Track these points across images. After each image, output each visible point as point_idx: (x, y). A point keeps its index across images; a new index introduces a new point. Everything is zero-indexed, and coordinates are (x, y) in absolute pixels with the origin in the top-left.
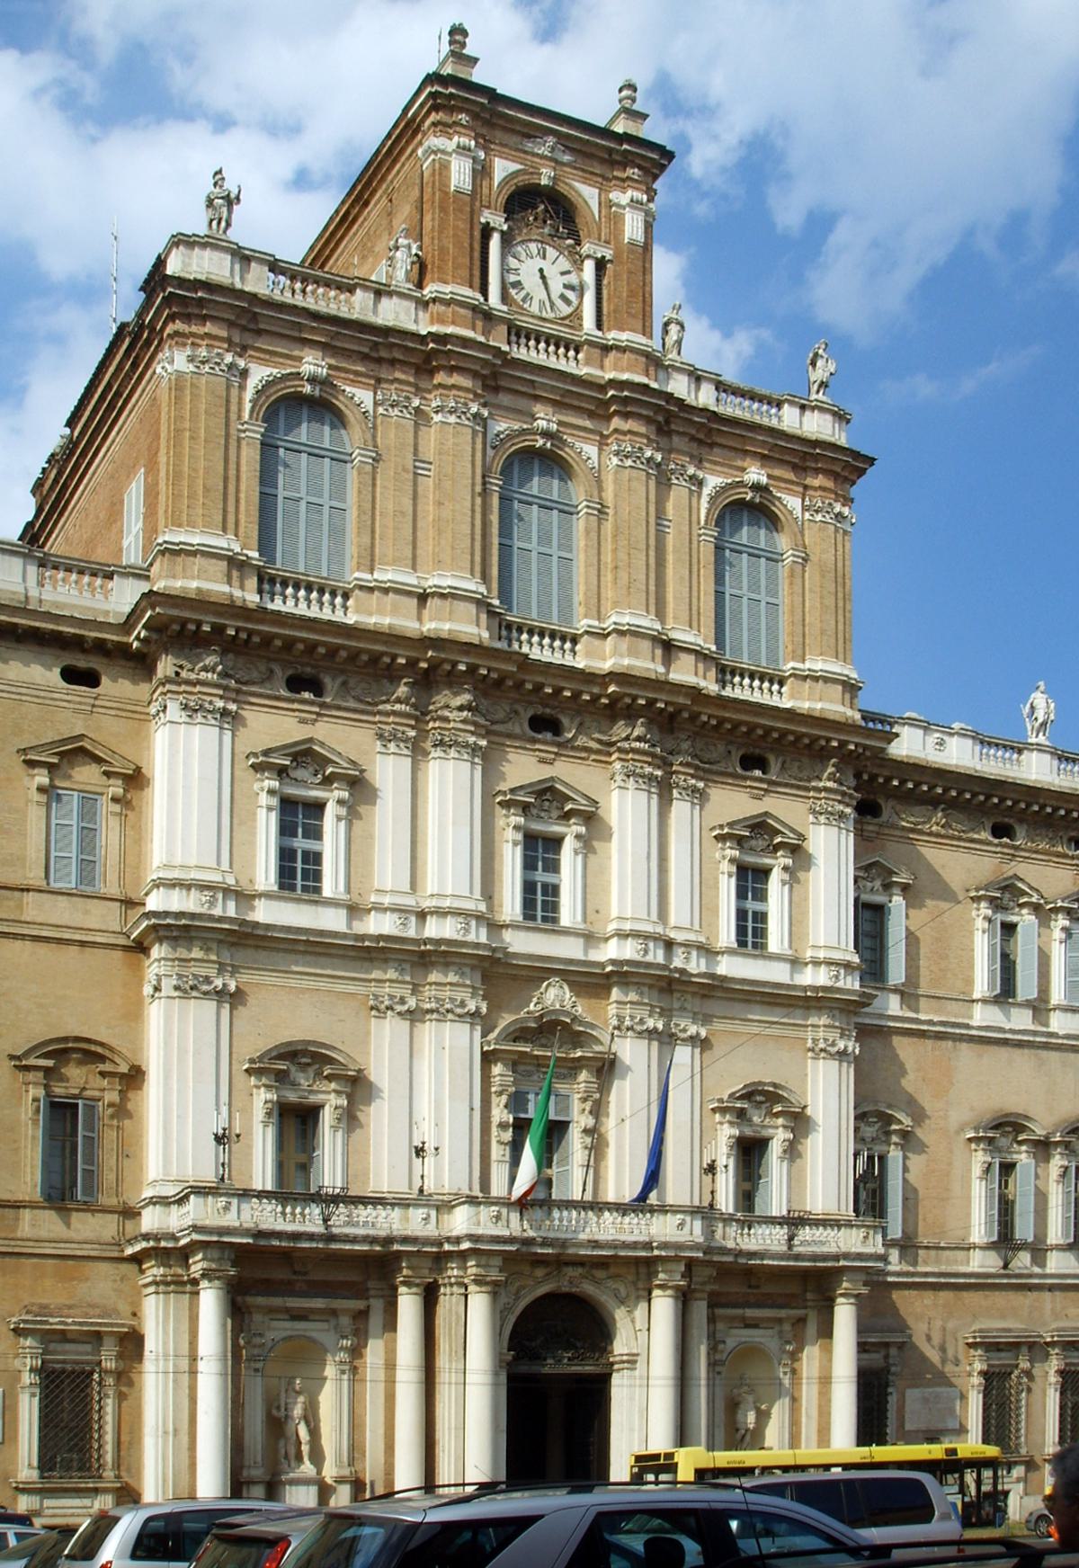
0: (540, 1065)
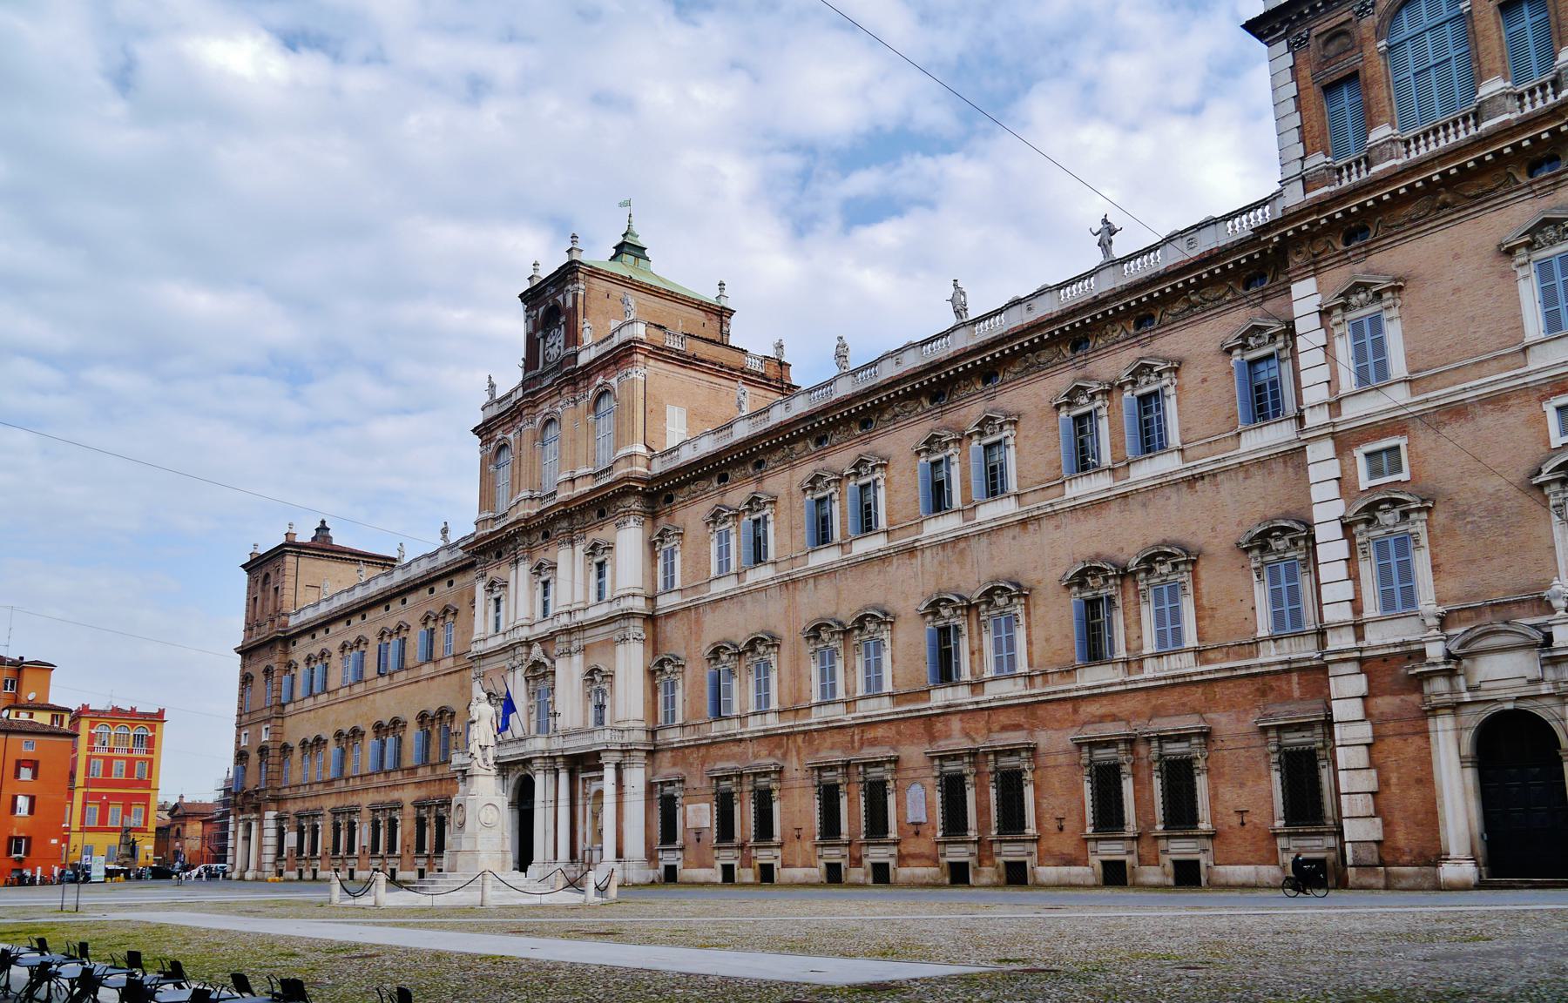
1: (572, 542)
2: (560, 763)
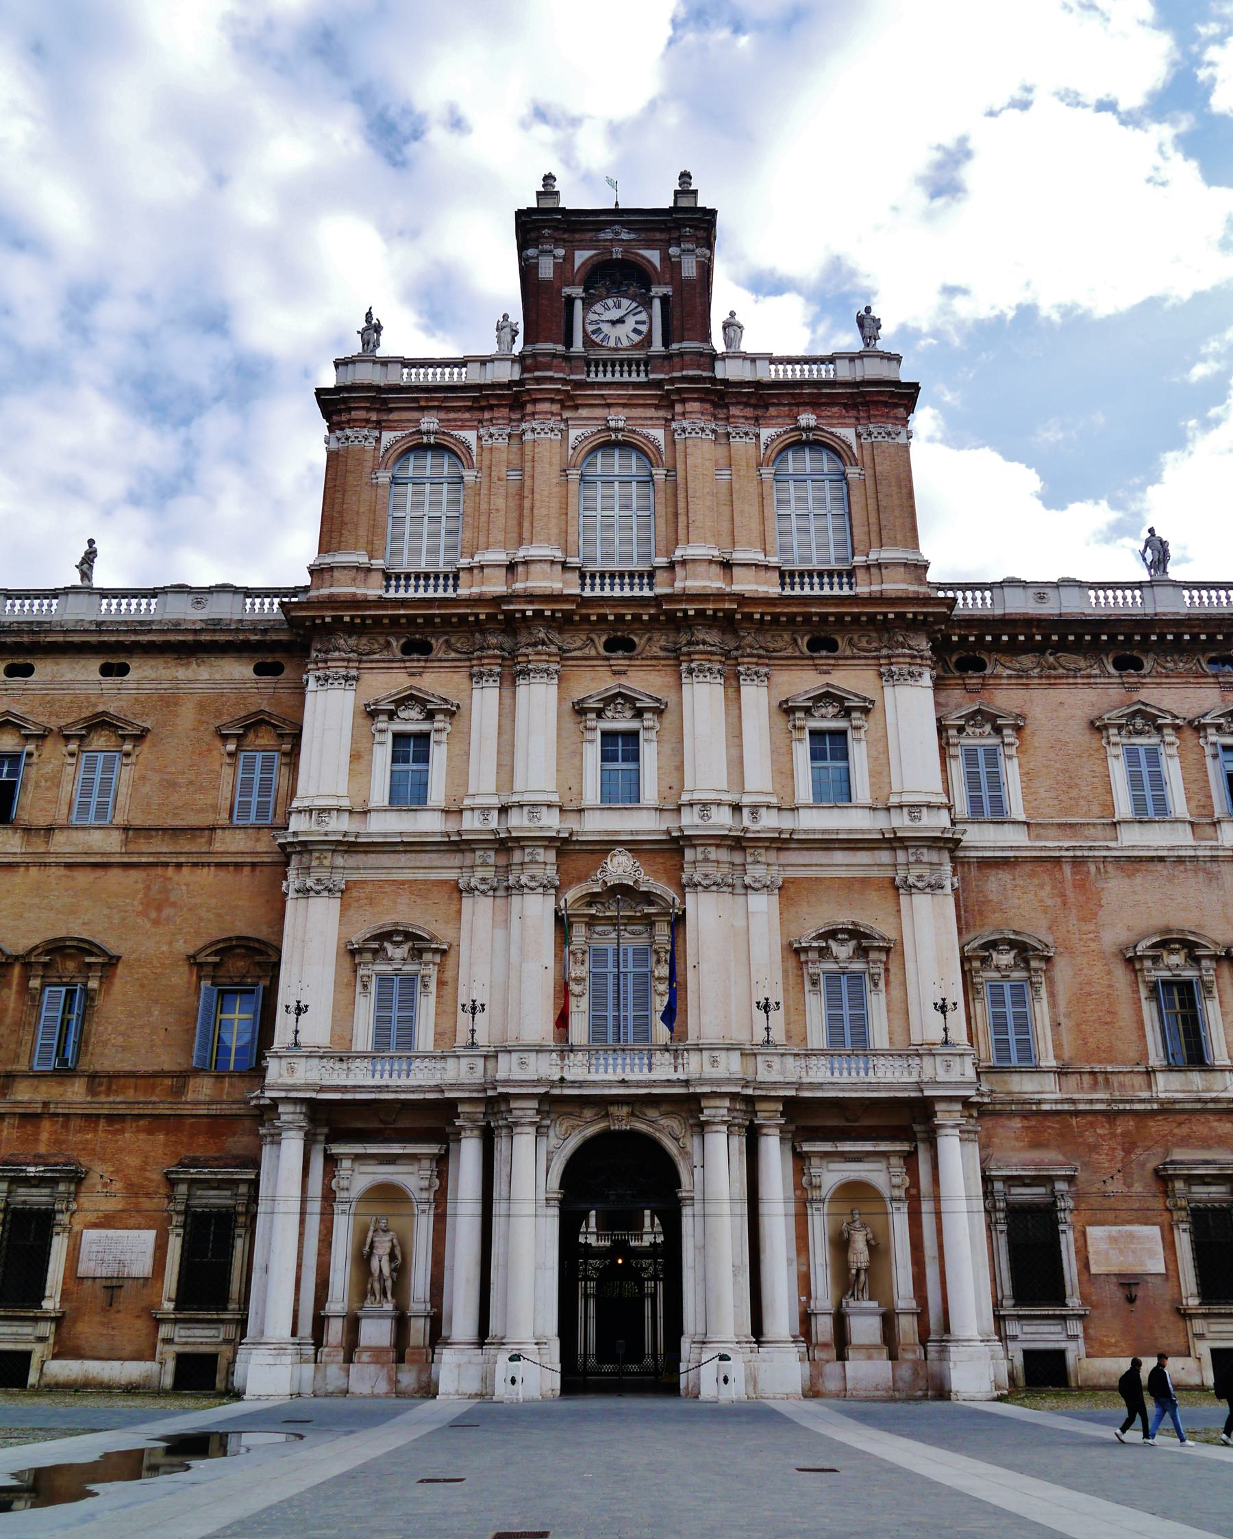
1: (733, 681)
2: (770, 1118)
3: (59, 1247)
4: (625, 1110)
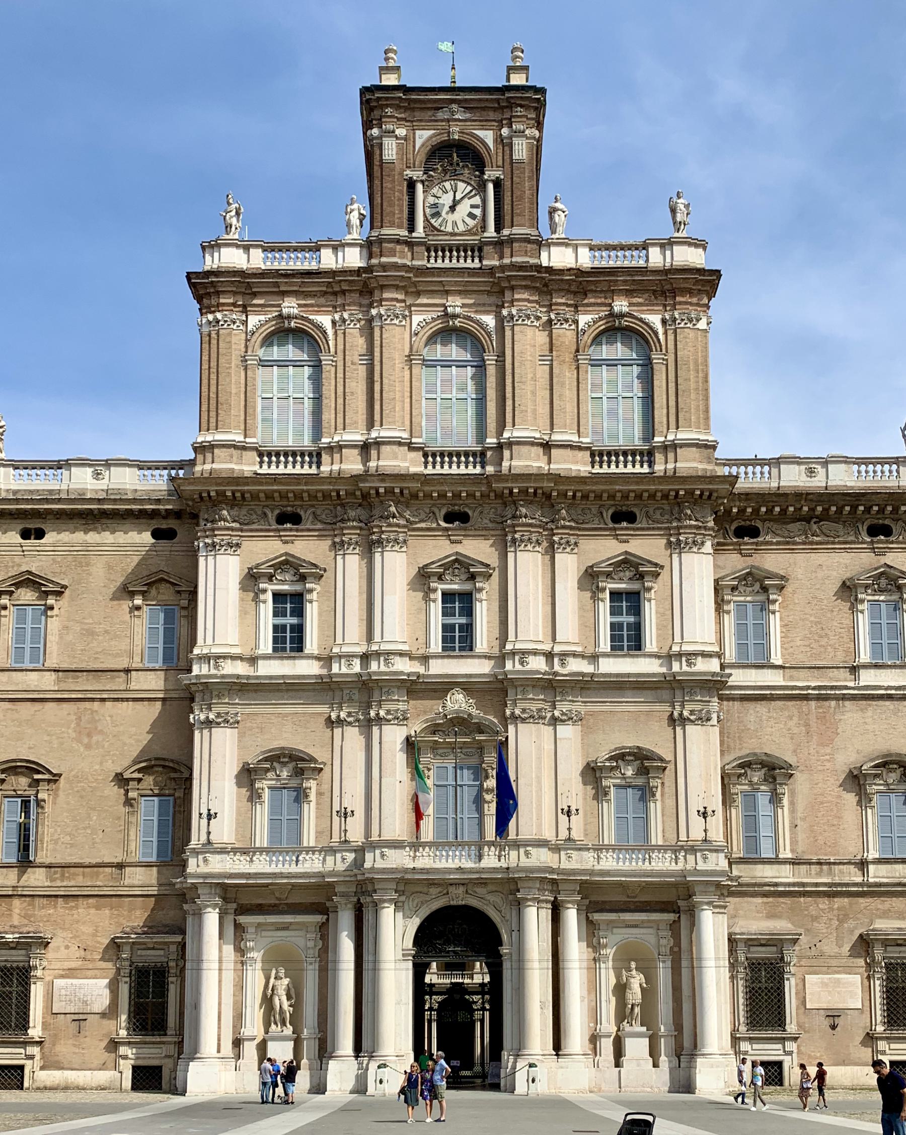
0: (471, 745)
3: (37, 992)
4: (461, 889)
